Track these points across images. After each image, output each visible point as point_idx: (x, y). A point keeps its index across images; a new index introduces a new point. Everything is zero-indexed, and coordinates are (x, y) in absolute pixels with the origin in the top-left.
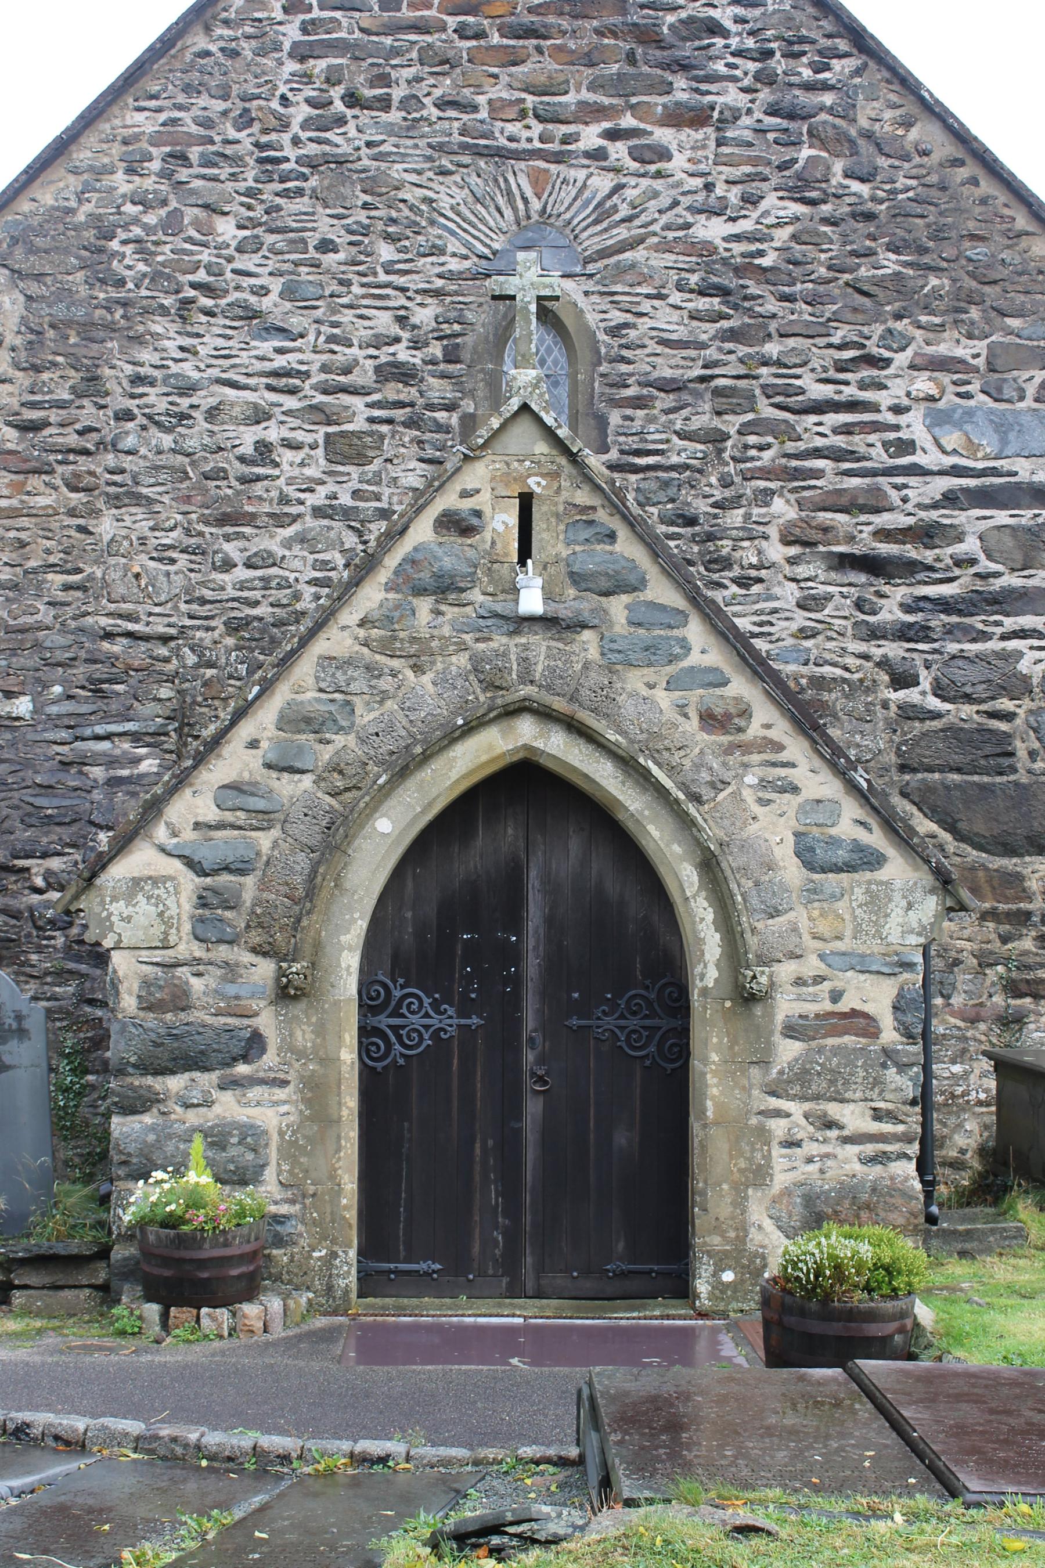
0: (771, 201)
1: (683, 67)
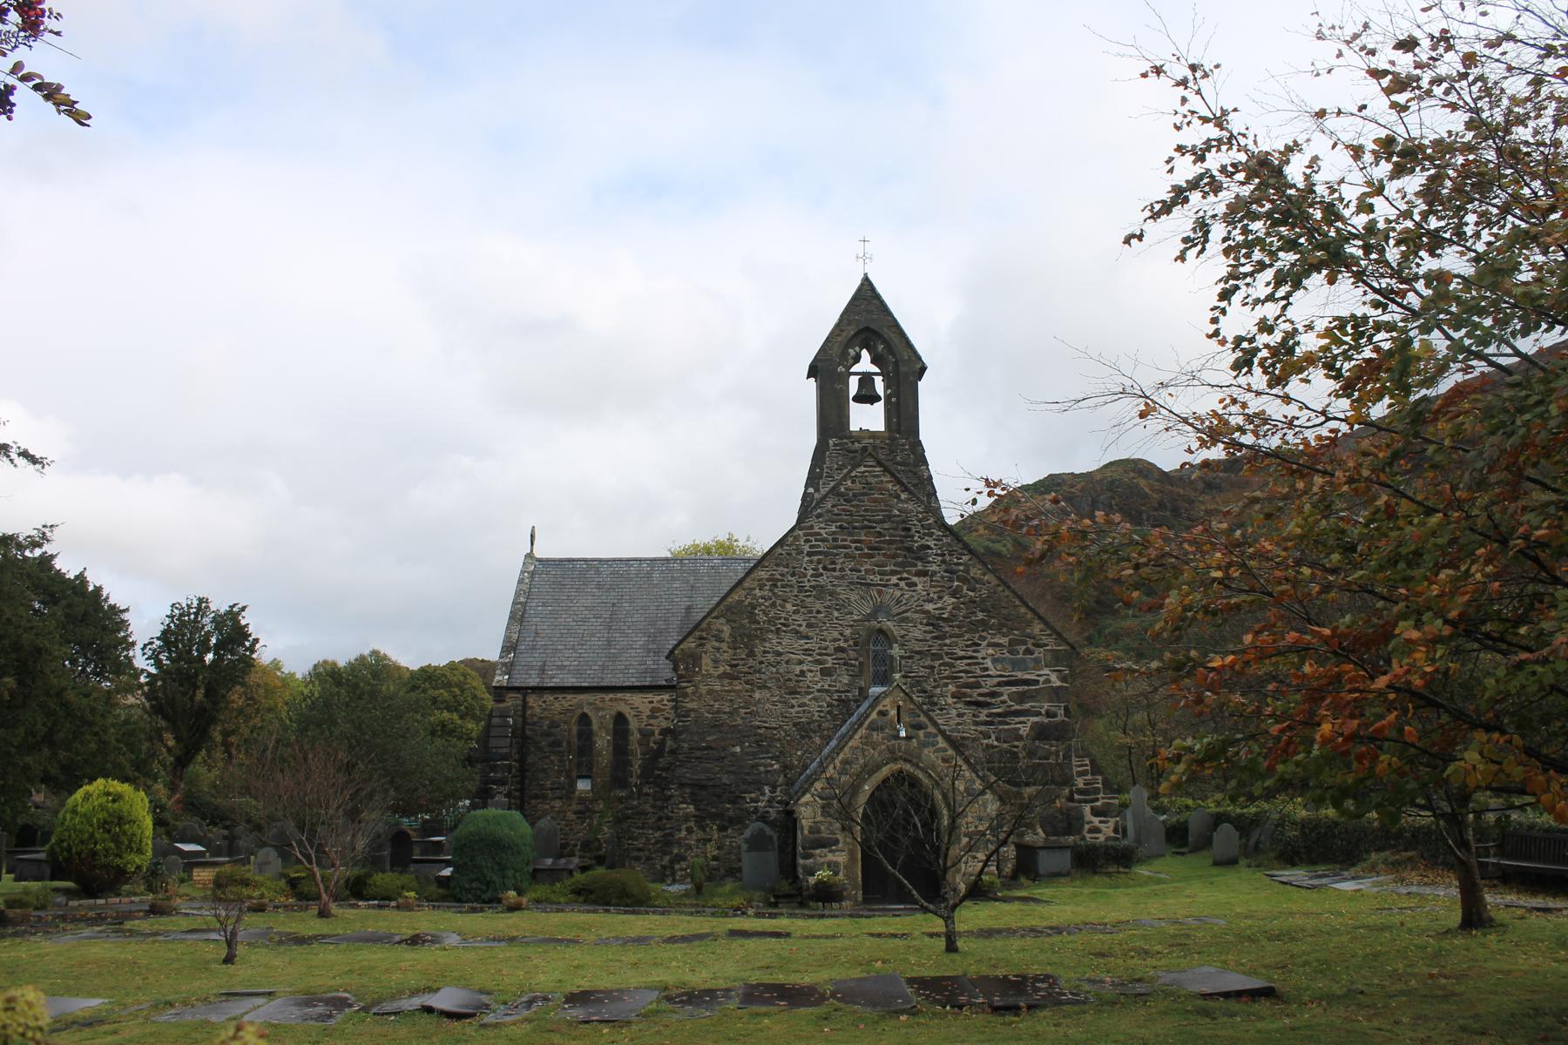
0: (946, 598)
1: (920, 559)
